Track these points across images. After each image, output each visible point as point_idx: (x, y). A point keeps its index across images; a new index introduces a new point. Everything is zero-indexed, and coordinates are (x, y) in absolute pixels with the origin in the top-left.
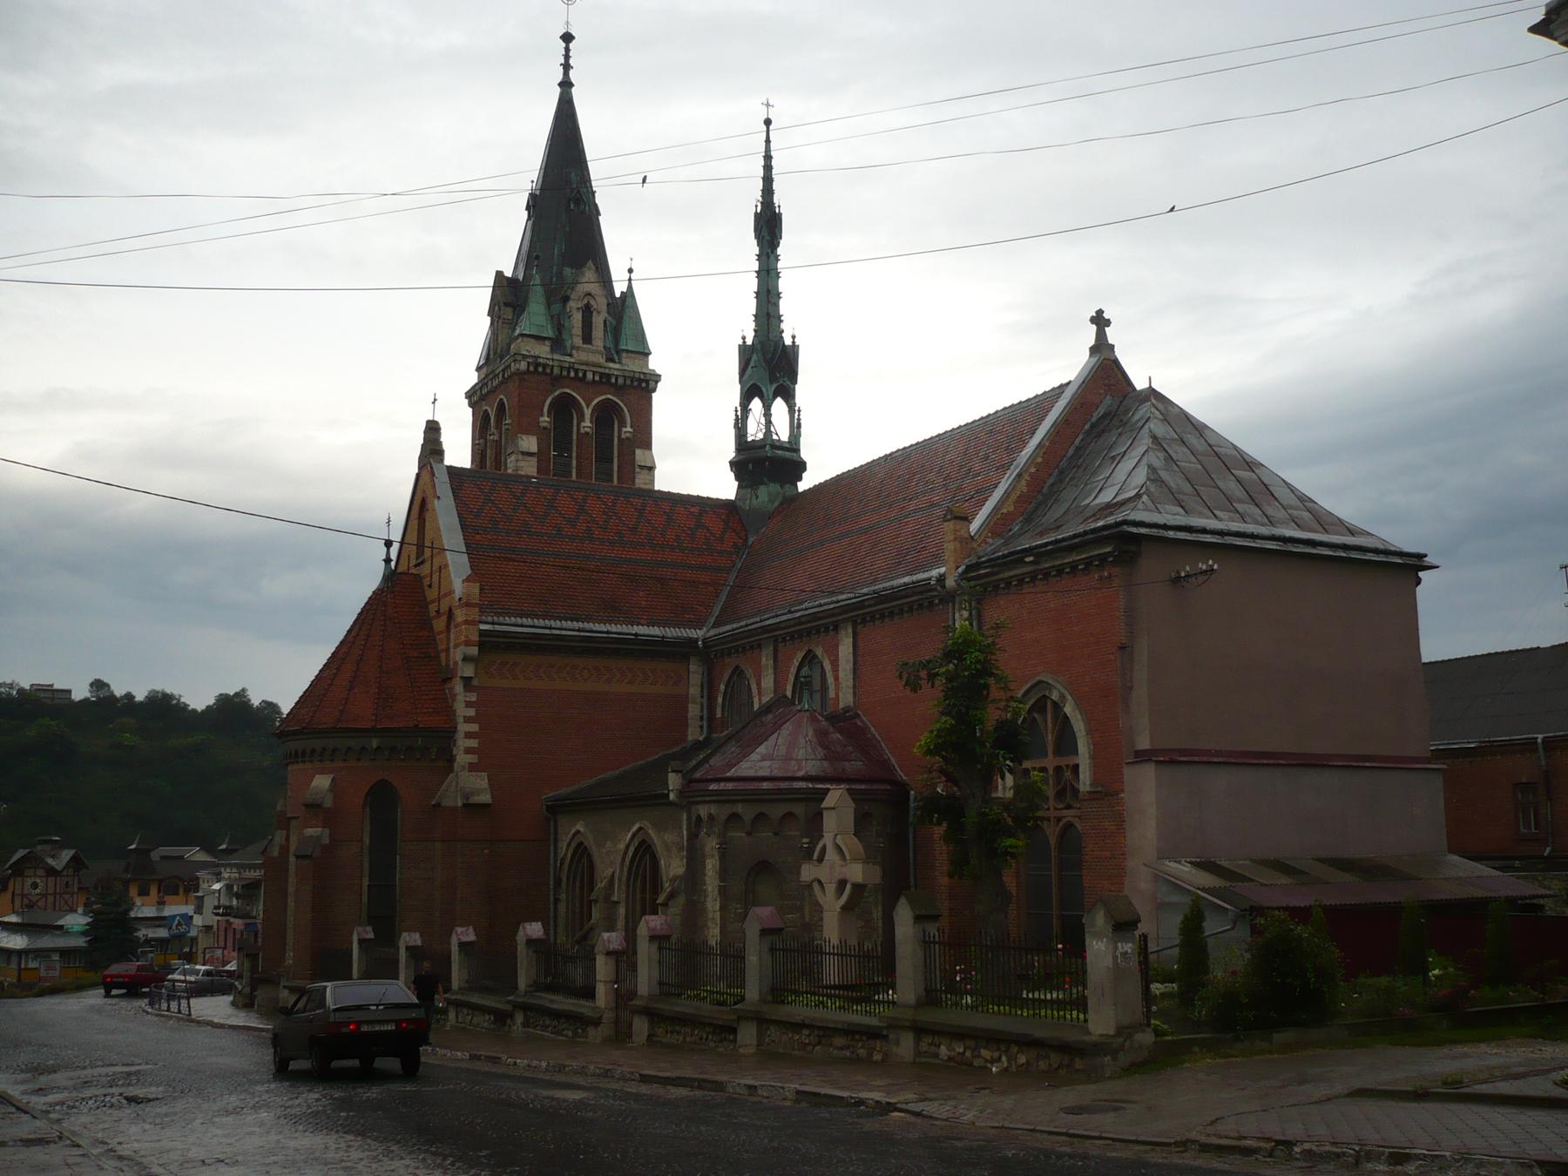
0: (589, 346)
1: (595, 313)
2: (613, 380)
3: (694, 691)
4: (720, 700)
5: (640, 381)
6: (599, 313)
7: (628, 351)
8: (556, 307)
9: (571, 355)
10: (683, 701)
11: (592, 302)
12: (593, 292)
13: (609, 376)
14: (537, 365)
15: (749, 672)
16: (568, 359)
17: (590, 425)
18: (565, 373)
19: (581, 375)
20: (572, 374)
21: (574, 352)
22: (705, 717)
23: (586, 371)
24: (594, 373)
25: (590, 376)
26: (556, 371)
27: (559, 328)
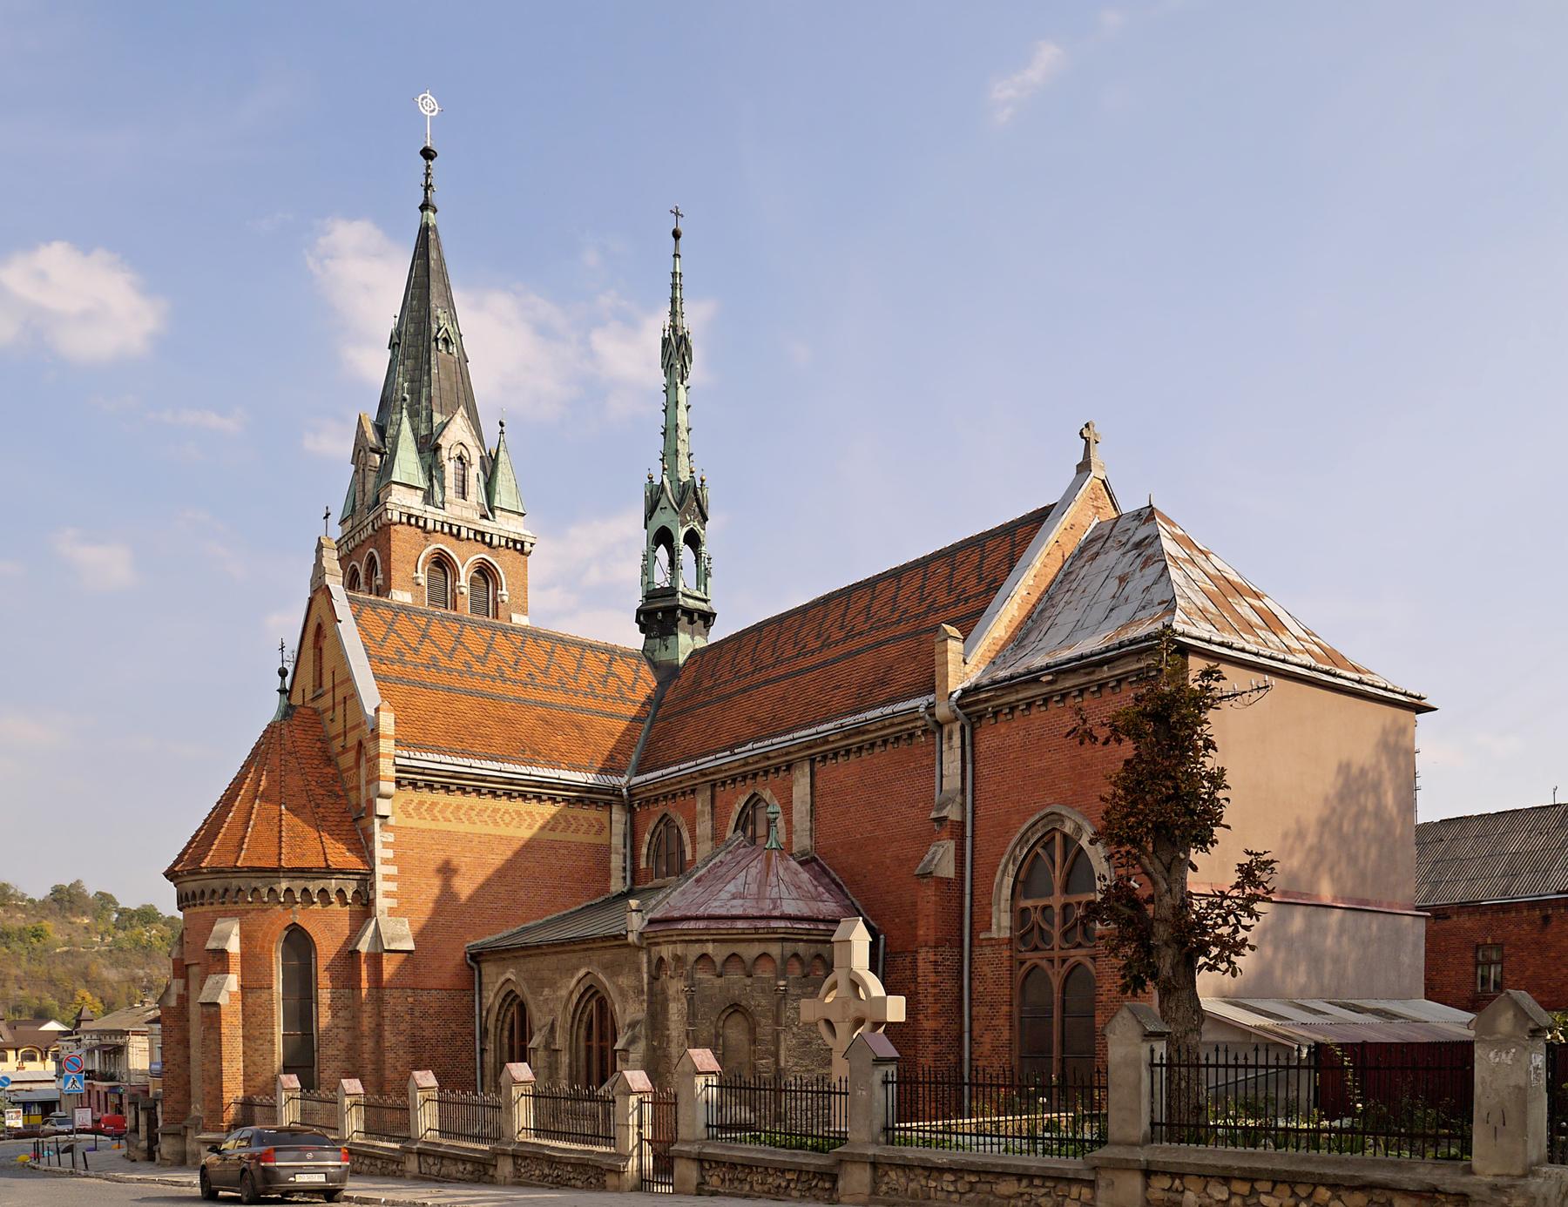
2: (487, 539)
3: (617, 841)
4: (644, 850)
5: (515, 542)
7: (502, 509)
10: (607, 850)
13: (483, 534)
14: (410, 516)
15: (680, 820)
18: (438, 527)
19: (455, 530)
22: (628, 868)
23: (460, 527)
25: (464, 533)
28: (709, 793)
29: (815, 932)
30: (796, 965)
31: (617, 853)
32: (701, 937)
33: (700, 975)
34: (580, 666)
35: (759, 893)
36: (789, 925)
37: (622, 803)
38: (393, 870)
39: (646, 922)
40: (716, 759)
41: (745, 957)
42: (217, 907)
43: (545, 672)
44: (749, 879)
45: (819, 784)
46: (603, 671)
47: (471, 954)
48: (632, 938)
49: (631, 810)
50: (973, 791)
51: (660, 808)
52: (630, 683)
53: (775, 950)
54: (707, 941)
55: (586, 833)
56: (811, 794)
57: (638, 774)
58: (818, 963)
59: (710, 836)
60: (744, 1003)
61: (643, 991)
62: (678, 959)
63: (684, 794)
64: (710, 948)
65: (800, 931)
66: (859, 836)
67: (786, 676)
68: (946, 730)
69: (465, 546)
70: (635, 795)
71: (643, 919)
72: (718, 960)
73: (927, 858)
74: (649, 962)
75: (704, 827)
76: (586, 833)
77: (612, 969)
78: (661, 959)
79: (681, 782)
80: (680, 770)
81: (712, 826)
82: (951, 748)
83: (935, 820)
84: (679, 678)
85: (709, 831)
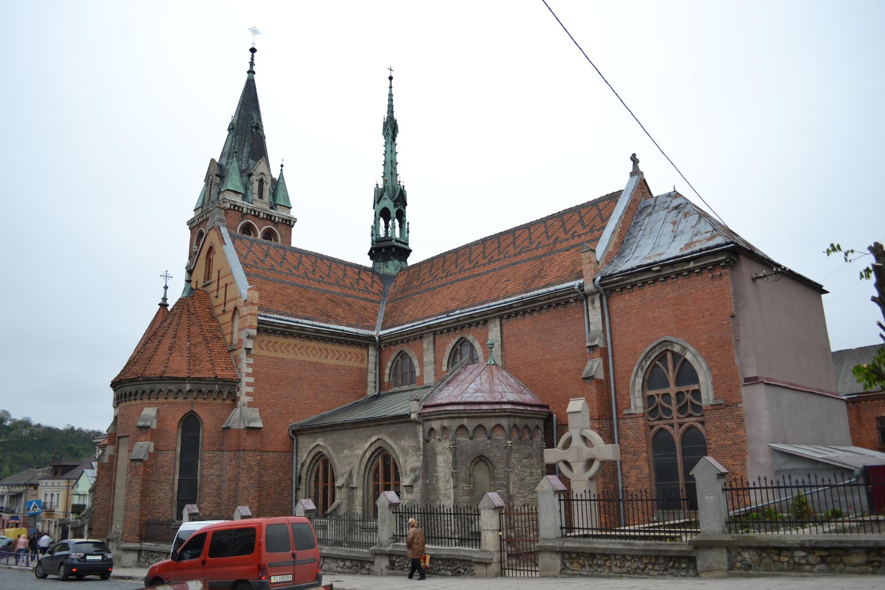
1: (265, 184)
2: (273, 219)
3: (371, 366)
4: (387, 371)
6: (267, 183)
8: (245, 179)
9: (252, 203)
10: (366, 371)
11: (264, 178)
12: (265, 173)
13: (271, 216)
15: (412, 354)
16: (251, 205)
19: (257, 214)
20: (253, 213)
21: (254, 202)
22: (378, 381)
24: (264, 213)
25: (261, 215)
26: (245, 210)
27: (246, 188)
28: (432, 338)
29: (526, 412)
30: (515, 431)
31: (372, 373)
32: (460, 415)
33: (459, 438)
34: (345, 275)
35: (491, 389)
36: (513, 407)
37: (375, 345)
39: (422, 407)
40: (437, 319)
41: (487, 427)
43: (328, 276)
44: (483, 381)
45: (505, 331)
46: (356, 277)
47: (292, 430)
48: (413, 416)
49: (379, 349)
50: (611, 331)
52: (370, 284)
53: (504, 422)
54: (464, 417)
55: (355, 361)
56: (501, 336)
57: (382, 329)
58: (526, 431)
59: (433, 362)
60: (486, 455)
61: (420, 448)
62: (444, 428)
63: (415, 339)
64: (465, 422)
65: (518, 411)
67: (470, 277)
68: (590, 298)
69: (262, 222)
70: (382, 341)
71: (420, 405)
72: (471, 429)
73: (587, 368)
74: (424, 431)
75: (429, 357)
77: (396, 437)
78: (432, 430)
79: (413, 333)
80: (413, 326)
81: (434, 356)
82: (594, 308)
83: (589, 347)
84: (396, 282)
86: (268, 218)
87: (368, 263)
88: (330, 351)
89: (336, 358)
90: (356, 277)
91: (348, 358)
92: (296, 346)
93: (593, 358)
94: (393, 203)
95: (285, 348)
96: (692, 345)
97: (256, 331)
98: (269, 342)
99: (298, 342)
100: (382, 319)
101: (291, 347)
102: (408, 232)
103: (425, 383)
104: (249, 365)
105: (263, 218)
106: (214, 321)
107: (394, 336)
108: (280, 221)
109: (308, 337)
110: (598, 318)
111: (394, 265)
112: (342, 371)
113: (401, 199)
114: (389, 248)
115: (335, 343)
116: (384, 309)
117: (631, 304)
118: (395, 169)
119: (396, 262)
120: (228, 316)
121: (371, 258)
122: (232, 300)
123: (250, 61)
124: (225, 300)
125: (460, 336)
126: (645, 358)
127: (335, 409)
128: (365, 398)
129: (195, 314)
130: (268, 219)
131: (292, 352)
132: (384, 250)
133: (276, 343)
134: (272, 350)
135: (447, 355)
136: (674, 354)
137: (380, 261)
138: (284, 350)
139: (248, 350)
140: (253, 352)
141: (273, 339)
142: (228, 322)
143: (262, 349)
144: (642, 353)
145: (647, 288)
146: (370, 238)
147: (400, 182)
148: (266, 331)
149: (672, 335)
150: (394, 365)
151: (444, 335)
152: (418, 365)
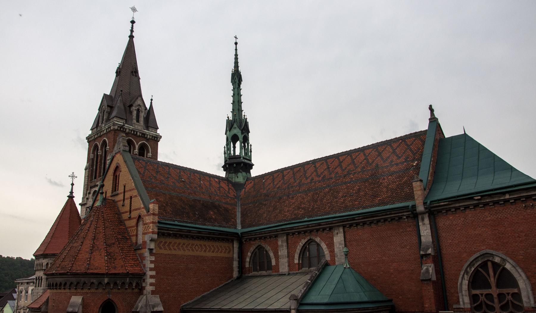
0: (138, 123)
1: (140, 112)
2: (146, 136)
3: (236, 256)
4: (248, 260)
6: (142, 112)
10: (232, 259)
11: (140, 108)
13: (144, 134)
15: (268, 248)
17: (137, 151)
19: (135, 133)
20: (132, 132)
23: (137, 132)
24: (140, 133)
25: (138, 134)
28: (285, 238)
38: (153, 273)
42: (73, 290)
45: (348, 237)
46: (218, 186)
51: (257, 243)
55: (225, 252)
56: (345, 241)
59: (287, 256)
66: (373, 259)
75: (283, 252)
76: (225, 252)
79: (270, 233)
81: (288, 252)
85: (286, 253)
86: (143, 136)
87: (222, 174)
88: (207, 246)
89: (211, 251)
90: (218, 186)
91: (220, 251)
92: (184, 244)
93: (426, 264)
94: (240, 131)
95: (177, 246)
96: (511, 258)
97: (157, 235)
98: (166, 243)
99: (186, 241)
100: (240, 218)
101: (181, 246)
102: (251, 152)
103: (280, 271)
104: (152, 262)
105: (140, 136)
106: (122, 225)
107: (254, 234)
108: (151, 137)
109: (193, 237)
110: (428, 232)
111: (242, 175)
112: (217, 261)
113: (245, 129)
114: (238, 164)
115: (211, 240)
116: (240, 211)
117: (454, 223)
118: (241, 106)
119: (244, 174)
120: (133, 222)
121: (224, 170)
122: (136, 210)
123: (129, 34)
124: (130, 208)
125: (309, 238)
126: (470, 266)
127: (212, 290)
128: (232, 279)
129: (108, 219)
130: (143, 137)
131: (181, 249)
132: (235, 165)
133: (170, 243)
134: (167, 248)
135: (298, 251)
136: (494, 264)
137: (232, 173)
138: (176, 248)
139: (151, 250)
140: (154, 251)
141: (169, 240)
142: (133, 227)
143: (161, 248)
144: (466, 261)
145: (468, 211)
146: (223, 155)
147: (244, 116)
148: (163, 234)
149: (492, 249)
150: (253, 255)
151: (295, 236)
152: (273, 257)
